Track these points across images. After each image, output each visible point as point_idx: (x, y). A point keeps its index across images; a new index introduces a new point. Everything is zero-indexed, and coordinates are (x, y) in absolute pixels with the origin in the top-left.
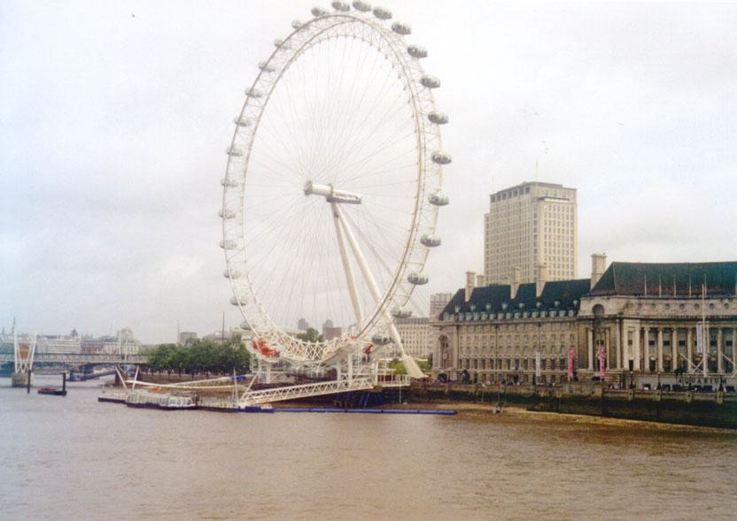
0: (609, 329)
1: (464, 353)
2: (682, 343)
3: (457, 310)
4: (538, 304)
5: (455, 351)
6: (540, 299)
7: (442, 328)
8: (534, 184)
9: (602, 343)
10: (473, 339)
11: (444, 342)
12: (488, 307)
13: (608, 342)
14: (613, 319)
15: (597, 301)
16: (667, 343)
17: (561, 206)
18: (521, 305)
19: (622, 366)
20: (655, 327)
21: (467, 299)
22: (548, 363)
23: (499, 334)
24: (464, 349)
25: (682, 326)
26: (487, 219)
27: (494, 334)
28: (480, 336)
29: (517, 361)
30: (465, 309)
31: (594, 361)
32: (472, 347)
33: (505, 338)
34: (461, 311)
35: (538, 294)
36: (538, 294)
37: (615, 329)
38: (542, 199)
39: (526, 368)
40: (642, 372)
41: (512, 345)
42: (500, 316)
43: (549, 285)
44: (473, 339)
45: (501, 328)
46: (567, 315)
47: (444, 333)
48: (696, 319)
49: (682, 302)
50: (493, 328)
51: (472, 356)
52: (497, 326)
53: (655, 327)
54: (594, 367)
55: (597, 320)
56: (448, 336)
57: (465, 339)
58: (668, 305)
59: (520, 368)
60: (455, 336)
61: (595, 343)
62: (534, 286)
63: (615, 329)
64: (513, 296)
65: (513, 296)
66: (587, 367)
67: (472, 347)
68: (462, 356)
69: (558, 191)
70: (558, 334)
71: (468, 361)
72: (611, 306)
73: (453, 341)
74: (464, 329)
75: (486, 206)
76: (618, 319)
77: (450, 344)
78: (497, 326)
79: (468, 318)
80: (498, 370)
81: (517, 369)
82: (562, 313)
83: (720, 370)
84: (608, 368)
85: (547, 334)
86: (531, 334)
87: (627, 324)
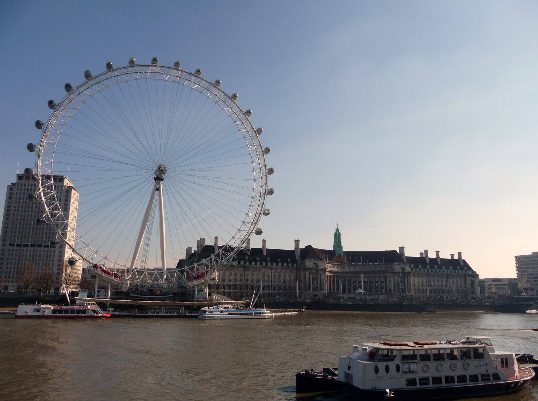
0: (321, 274)
9: (314, 279)
10: (227, 274)
13: (319, 279)
15: (316, 261)
22: (277, 288)
26: (11, 189)
28: (233, 273)
32: (227, 277)
33: (250, 275)
36: (265, 253)
41: (254, 278)
43: (269, 251)
44: (227, 274)
50: (242, 269)
52: (244, 268)
66: (310, 290)
75: (14, 180)
80: (245, 291)
85: (276, 274)
86: (267, 274)
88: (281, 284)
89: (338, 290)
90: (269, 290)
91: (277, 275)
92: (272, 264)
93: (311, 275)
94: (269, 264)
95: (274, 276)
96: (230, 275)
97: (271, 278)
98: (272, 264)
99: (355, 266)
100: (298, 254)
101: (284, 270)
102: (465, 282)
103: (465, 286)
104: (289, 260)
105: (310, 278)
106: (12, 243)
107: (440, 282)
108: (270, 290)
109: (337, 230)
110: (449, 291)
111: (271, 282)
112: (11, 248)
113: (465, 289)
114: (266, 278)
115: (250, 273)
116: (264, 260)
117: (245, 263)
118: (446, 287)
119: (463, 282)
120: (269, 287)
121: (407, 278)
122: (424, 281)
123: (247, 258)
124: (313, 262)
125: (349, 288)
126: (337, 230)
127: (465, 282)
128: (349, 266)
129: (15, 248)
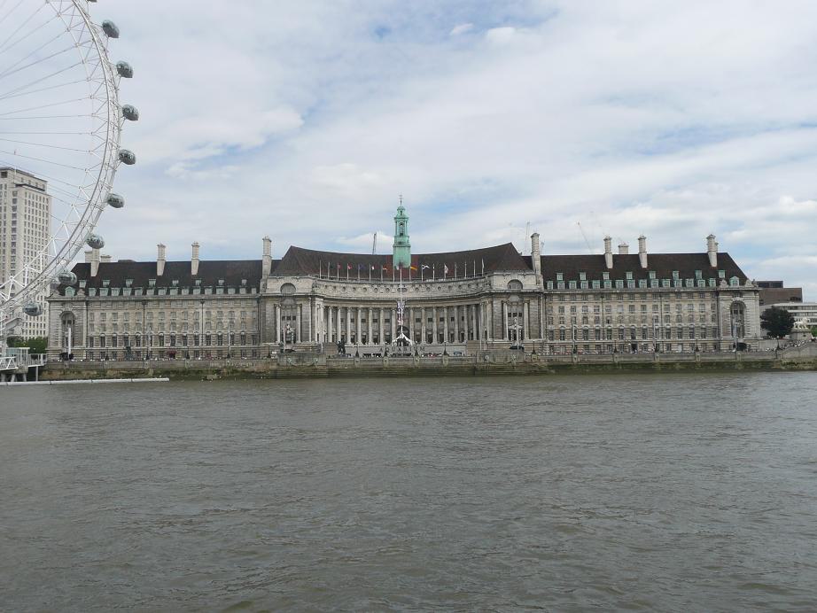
0: (301, 306)
1: (96, 330)
2: (387, 321)
3: (83, 284)
4: (198, 282)
5: (85, 332)
6: (198, 276)
7: (64, 303)
8: (12, 170)
10: (109, 315)
11: (67, 319)
12: (129, 283)
14: (306, 297)
15: (289, 279)
16: (387, 321)
17: (39, 195)
18: (175, 282)
19: (313, 339)
20: (333, 306)
21: (94, 273)
22: (213, 338)
24: (95, 326)
25: (345, 306)
27: (141, 311)
28: (120, 313)
29: (173, 338)
30: (95, 283)
31: (282, 335)
33: (155, 316)
34: (88, 286)
35: (194, 271)
36: (194, 271)
37: (307, 307)
38: (20, 185)
39: (185, 344)
40: (326, 344)
42: (150, 293)
44: (109, 315)
45: (150, 304)
46: (121, 293)
47: (68, 308)
48: (394, 301)
49: (344, 285)
50: (139, 305)
51: (108, 333)
53: (333, 306)
54: (282, 340)
55: (288, 300)
56: (75, 313)
57: (97, 314)
58: (335, 287)
59: (178, 345)
60: (85, 311)
61: (283, 318)
62: (189, 264)
63: (307, 307)
64: (160, 272)
65: (160, 272)
66: (276, 340)
67: (108, 323)
68: (92, 334)
69: (32, 180)
70: (226, 312)
71: (232, 336)
72: (303, 285)
73: (82, 318)
74: (92, 306)
76: (311, 298)
77: (77, 321)
78: (145, 302)
79: (104, 293)
81: (173, 344)
82: (231, 291)
83: (423, 342)
84: (299, 341)
85: (212, 311)
87: (318, 301)
88: (223, 331)
89: (344, 337)
90: (197, 343)
91: (214, 313)
92: (203, 292)
93: (278, 310)
97: (202, 319)
99: (429, 286)
100: (267, 267)
101: (232, 304)
102: (716, 307)
103: (715, 318)
104: (244, 281)
107: (638, 311)
108: (200, 344)
109: (401, 210)
110: (665, 331)
111: (201, 328)
113: (714, 324)
114: (191, 321)
115: (156, 313)
117: (145, 293)
118: (657, 321)
119: (708, 307)
120: (196, 337)
121: (529, 304)
122: (591, 309)
123: (152, 282)
124: (282, 282)
125: (388, 334)
126: (401, 210)
127: (716, 307)
128: (417, 286)
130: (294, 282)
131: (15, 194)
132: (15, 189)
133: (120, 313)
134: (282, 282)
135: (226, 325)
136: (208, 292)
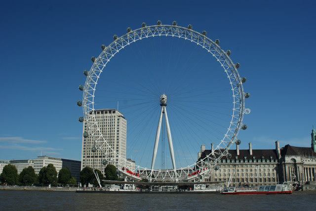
15: (294, 157)
23: (236, 169)
35: (251, 154)
36: (251, 154)
45: (237, 166)
52: (235, 165)
64: (238, 154)
65: (238, 154)
76: (302, 164)
78: (235, 165)
91: (262, 170)
92: (257, 161)
94: (255, 161)
95: (260, 170)
96: (225, 171)
97: (258, 172)
98: (257, 161)
105: (289, 171)
106: (89, 155)
112: (88, 159)
116: (250, 158)
123: (237, 158)
129: (91, 159)
130: (295, 158)
131: (118, 119)
132: (119, 118)
133: (227, 169)
134: (291, 158)
135: (267, 174)
136: (259, 161)
